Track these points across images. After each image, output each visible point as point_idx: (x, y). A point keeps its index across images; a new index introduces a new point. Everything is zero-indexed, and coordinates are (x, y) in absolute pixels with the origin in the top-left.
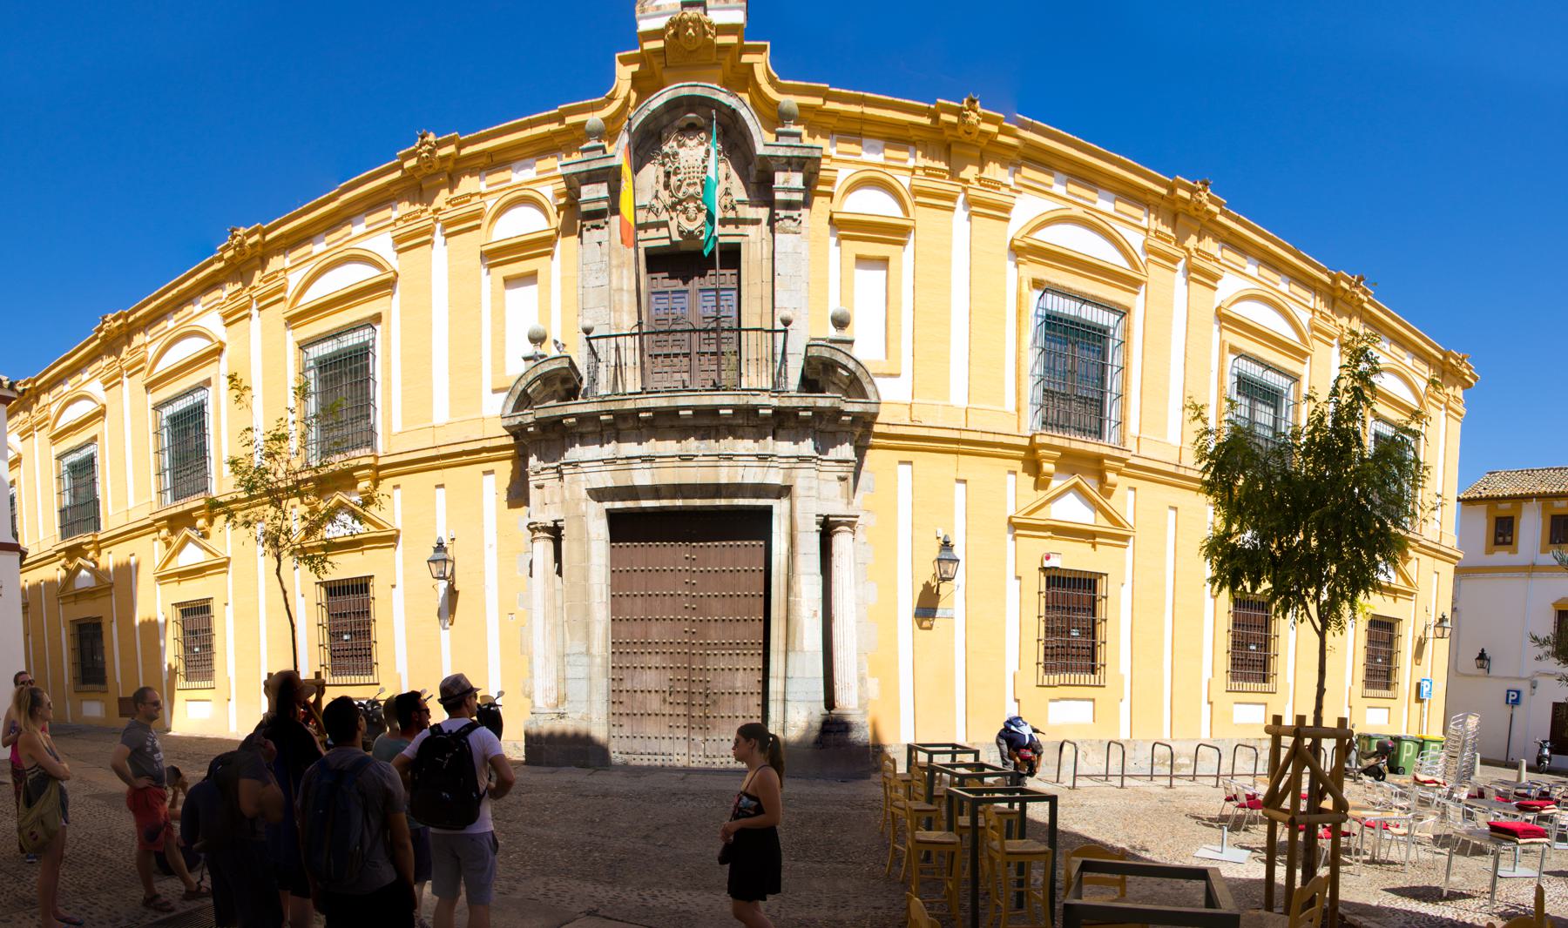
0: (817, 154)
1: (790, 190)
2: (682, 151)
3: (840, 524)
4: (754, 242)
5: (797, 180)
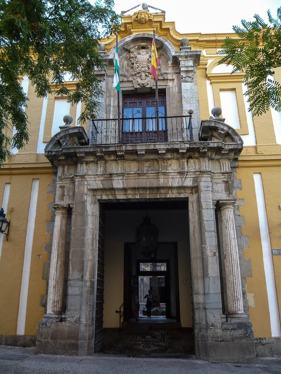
0: (199, 53)
1: (187, 67)
2: (138, 56)
3: (224, 204)
4: (172, 86)
5: (191, 63)
